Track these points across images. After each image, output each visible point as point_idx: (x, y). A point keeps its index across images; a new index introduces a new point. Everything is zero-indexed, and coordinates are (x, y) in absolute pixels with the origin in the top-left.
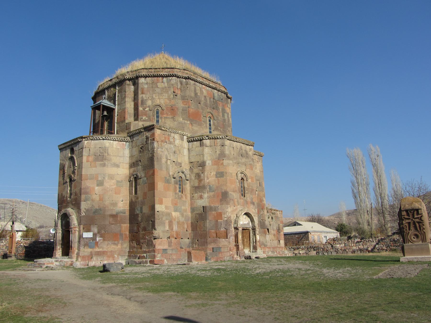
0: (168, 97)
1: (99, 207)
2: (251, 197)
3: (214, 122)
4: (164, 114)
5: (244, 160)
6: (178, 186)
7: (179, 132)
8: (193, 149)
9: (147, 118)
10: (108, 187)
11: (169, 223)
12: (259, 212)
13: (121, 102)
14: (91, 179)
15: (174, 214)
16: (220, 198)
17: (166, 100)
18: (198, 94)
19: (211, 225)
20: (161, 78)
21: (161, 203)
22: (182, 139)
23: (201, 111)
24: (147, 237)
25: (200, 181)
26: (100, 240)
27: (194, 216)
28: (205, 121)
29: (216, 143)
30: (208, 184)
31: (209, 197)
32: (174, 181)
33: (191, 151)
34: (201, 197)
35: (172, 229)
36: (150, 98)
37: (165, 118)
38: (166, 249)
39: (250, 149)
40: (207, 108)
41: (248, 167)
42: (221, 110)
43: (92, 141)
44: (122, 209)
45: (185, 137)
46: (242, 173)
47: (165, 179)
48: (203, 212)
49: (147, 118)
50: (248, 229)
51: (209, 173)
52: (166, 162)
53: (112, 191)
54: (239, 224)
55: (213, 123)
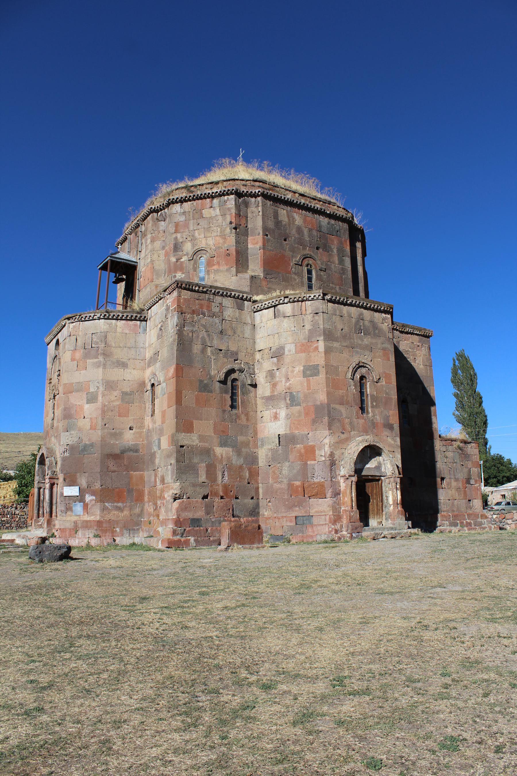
0: (221, 232)
1: (89, 440)
2: (386, 415)
3: (321, 275)
4: (214, 265)
5: (367, 341)
6: (228, 397)
7: (233, 293)
8: (262, 325)
9: (184, 275)
10: (106, 404)
11: (206, 467)
13: (145, 252)
14: (78, 391)
15: (219, 451)
16: (313, 416)
17: (218, 238)
18: (284, 223)
19: (295, 471)
20: (208, 200)
22: (241, 308)
23: (288, 253)
24: (166, 496)
25: (274, 385)
26: (91, 501)
27: (264, 455)
28: (298, 273)
29: (303, 308)
30: (288, 391)
31: (288, 417)
32: (220, 388)
33: (259, 328)
34: (276, 417)
39: (384, 319)
40: (304, 249)
41: (377, 354)
42: (335, 251)
44: (131, 443)
46: (365, 367)
47: (200, 385)
48: (279, 446)
49: (184, 275)
50: (377, 478)
51: (290, 369)
52: (203, 351)
53: (112, 411)
55: (317, 276)
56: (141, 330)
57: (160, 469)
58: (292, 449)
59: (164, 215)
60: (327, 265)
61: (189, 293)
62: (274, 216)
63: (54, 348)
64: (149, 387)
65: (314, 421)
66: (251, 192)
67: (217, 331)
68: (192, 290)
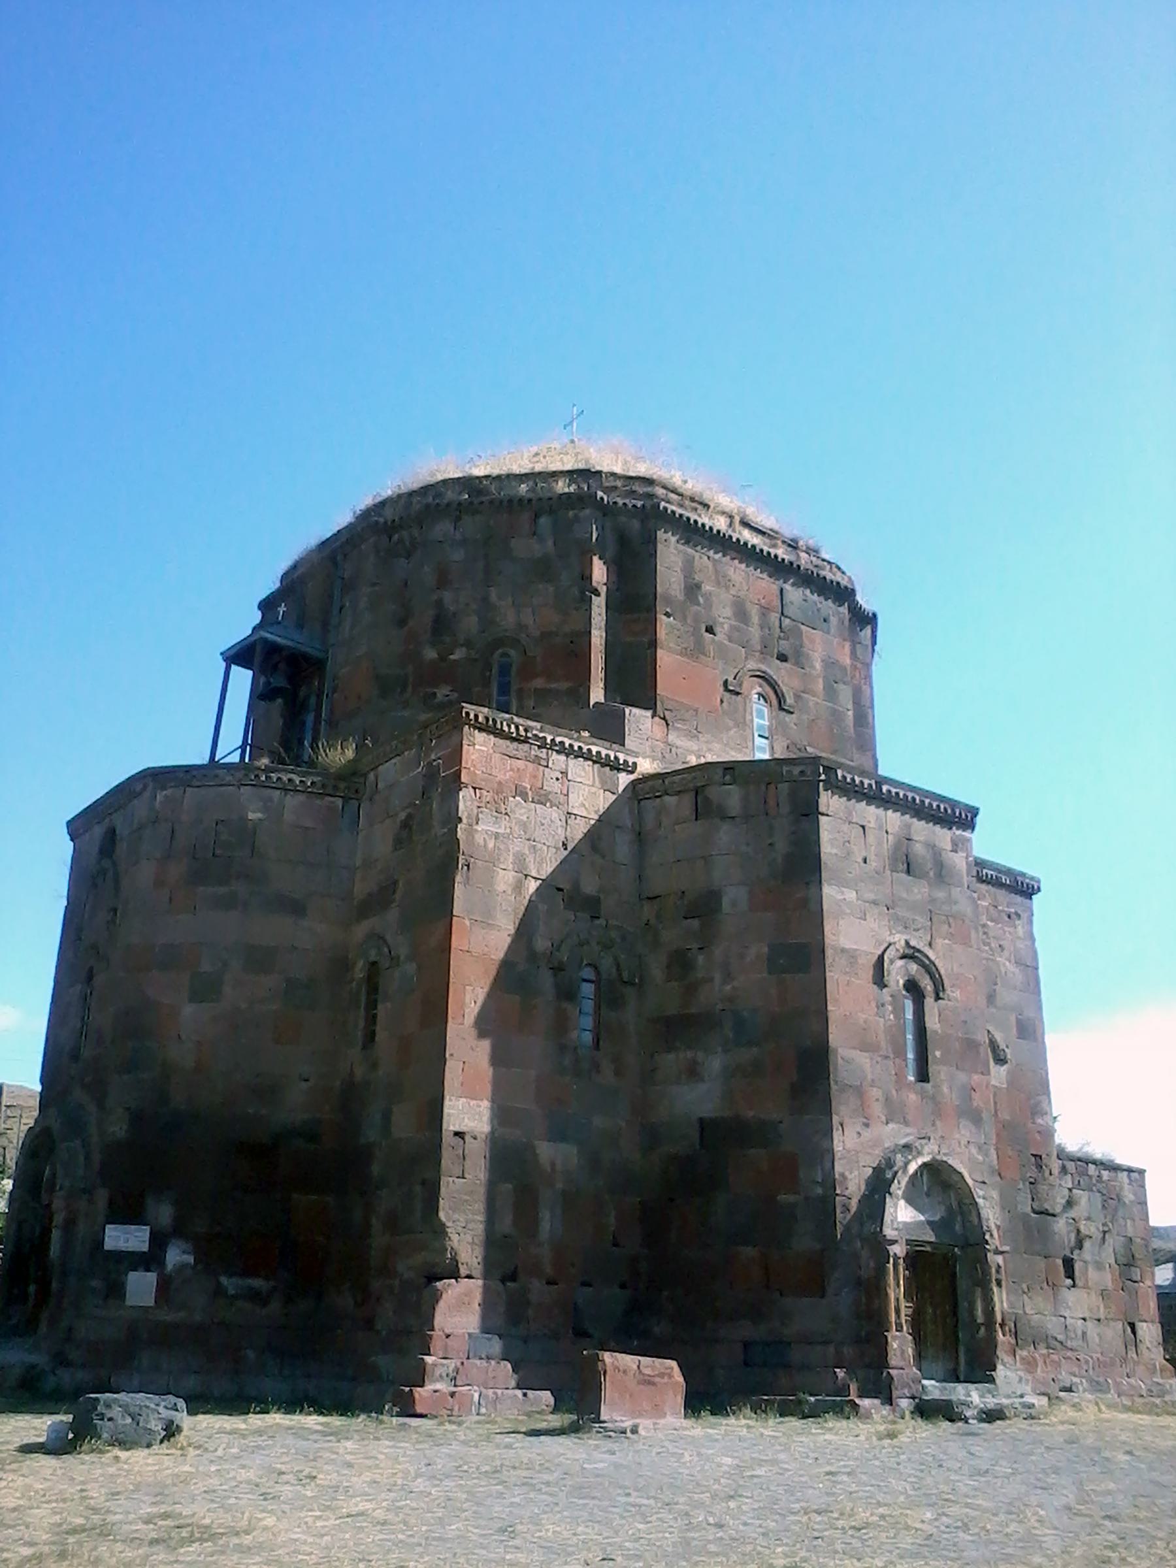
5: (919, 890)
7: (594, 749)
10: (244, 1006)
24: (401, 1267)
25: (691, 990)
29: (771, 802)
34: (693, 1072)
36: (474, 607)
37: (536, 690)
42: (818, 665)
54: (887, 1218)
64: (359, 972)
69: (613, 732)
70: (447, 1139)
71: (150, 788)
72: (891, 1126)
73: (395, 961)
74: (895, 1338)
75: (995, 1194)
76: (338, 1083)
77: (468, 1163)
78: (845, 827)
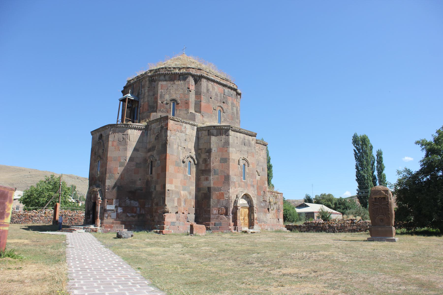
3: (224, 115)
4: (179, 107)
5: (246, 148)
6: (187, 169)
7: (191, 122)
8: (202, 137)
10: (129, 168)
12: (259, 194)
15: (182, 192)
21: (171, 183)
24: (159, 212)
35: (181, 205)
38: (174, 222)
43: (117, 128)
44: (139, 186)
45: (195, 127)
46: (244, 160)
48: (208, 191)
52: (178, 148)
56: (145, 134)
57: (155, 199)
58: (214, 193)
59: (155, 79)
60: (226, 110)
61: (173, 121)
62: (206, 87)
63: (98, 138)
65: (224, 183)
66: (198, 75)
67: (183, 140)
68: (174, 120)
69: (193, 118)
70: (167, 191)
71: (110, 128)
72: (239, 188)
73: (156, 160)
74: (238, 221)
75: (256, 199)
76: (145, 181)
77: (170, 195)
78: (234, 137)
